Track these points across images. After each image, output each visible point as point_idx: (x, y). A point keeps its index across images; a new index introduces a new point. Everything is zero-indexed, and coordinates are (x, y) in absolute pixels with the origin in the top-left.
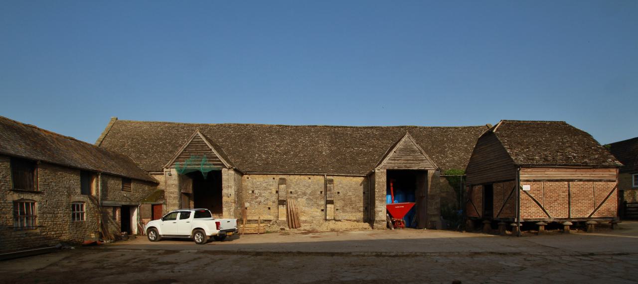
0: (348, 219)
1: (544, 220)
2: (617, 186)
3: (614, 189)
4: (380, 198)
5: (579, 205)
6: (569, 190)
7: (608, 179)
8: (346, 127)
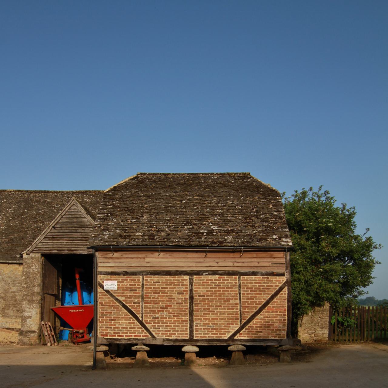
0: (10, 327)
1: (144, 342)
2: (287, 283)
3: (281, 289)
4: (29, 298)
5: (211, 316)
6: (191, 290)
7: (269, 270)
8: (48, 192)
